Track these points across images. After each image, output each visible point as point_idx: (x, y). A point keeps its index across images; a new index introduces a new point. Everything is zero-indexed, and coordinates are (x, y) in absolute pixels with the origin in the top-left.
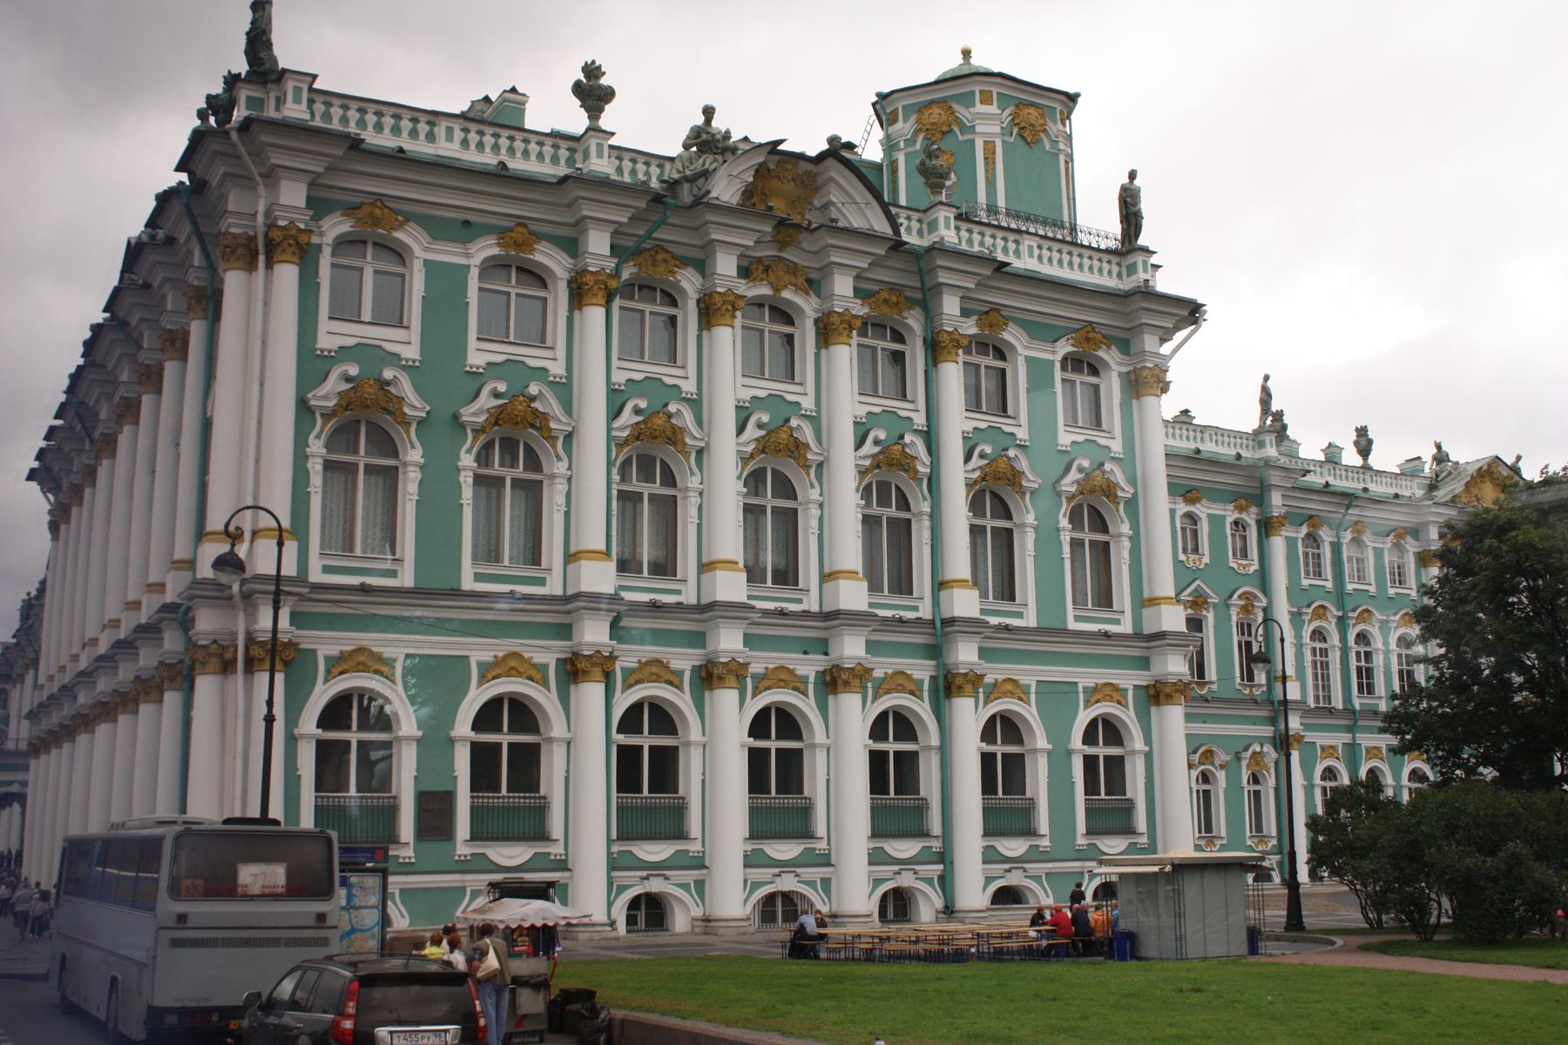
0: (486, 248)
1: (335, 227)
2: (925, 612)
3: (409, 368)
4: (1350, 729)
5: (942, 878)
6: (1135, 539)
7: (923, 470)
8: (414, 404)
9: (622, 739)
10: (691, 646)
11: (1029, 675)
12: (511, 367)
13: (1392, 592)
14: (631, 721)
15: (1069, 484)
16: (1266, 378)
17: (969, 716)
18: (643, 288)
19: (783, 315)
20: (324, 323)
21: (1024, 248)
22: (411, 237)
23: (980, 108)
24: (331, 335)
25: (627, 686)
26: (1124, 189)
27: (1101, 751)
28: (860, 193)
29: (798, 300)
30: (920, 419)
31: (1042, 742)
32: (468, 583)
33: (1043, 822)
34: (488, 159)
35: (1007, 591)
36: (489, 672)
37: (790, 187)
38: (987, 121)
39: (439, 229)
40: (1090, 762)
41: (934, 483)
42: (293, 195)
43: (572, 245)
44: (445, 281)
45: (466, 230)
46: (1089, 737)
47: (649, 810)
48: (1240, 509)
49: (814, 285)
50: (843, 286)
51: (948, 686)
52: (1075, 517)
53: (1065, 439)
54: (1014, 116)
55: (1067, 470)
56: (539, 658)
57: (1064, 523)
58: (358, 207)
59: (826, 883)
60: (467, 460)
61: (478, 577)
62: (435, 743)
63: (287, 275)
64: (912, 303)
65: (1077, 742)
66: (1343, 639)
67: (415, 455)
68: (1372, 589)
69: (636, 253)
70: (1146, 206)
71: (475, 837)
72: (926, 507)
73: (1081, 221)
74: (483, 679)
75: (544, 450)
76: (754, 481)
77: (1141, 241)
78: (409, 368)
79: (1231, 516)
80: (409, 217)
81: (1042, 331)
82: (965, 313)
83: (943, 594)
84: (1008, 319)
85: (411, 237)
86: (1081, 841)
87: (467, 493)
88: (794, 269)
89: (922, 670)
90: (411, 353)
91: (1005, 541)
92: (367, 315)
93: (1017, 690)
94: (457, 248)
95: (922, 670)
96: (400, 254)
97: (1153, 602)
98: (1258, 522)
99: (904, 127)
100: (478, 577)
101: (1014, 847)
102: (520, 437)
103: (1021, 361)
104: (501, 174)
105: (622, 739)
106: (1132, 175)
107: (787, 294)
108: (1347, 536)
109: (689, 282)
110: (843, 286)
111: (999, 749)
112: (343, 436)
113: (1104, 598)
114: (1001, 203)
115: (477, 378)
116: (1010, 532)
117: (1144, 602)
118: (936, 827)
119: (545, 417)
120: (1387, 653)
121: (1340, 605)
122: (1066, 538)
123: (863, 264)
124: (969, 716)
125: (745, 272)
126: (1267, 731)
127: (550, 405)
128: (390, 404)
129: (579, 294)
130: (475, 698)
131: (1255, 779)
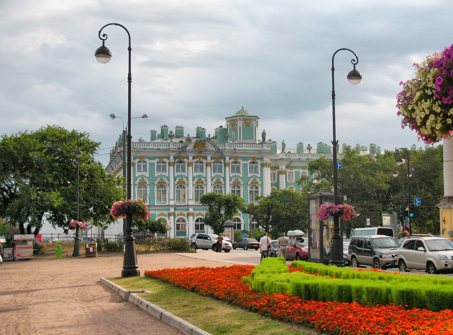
0: (157, 160)
3: (147, 178)
12: (161, 176)
14: (178, 221)
15: (249, 183)
18: (181, 162)
19: (201, 162)
22: (147, 160)
23: (239, 121)
30: (223, 176)
32: (156, 204)
36: (159, 215)
38: (240, 124)
39: (150, 158)
43: (169, 158)
44: (152, 165)
45: (154, 158)
47: (181, 232)
49: (205, 158)
50: (209, 158)
52: (252, 187)
56: (165, 213)
57: (249, 189)
60: (155, 189)
64: (221, 158)
67: (148, 189)
69: (178, 157)
72: (223, 189)
75: (166, 186)
76: (197, 187)
78: (147, 178)
80: (146, 157)
82: (230, 159)
84: (239, 158)
85: (147, 160)
87: (156, 193)
88: (202, 156)
90: (148, 175)
96: (146, 162)
102: (162, 185)
106: (264, 130)
107: (201, 160)
109: (186, 160)
110: (209, 158)
115: (157, 178)
122: (249, 191)
125: (194, 158)
127: (166, 180)
129: (170, 165)
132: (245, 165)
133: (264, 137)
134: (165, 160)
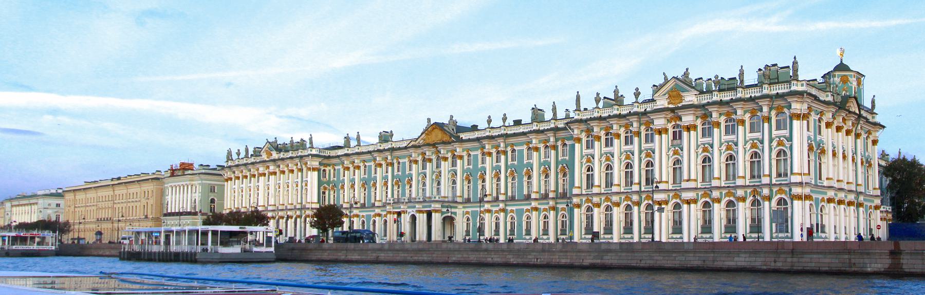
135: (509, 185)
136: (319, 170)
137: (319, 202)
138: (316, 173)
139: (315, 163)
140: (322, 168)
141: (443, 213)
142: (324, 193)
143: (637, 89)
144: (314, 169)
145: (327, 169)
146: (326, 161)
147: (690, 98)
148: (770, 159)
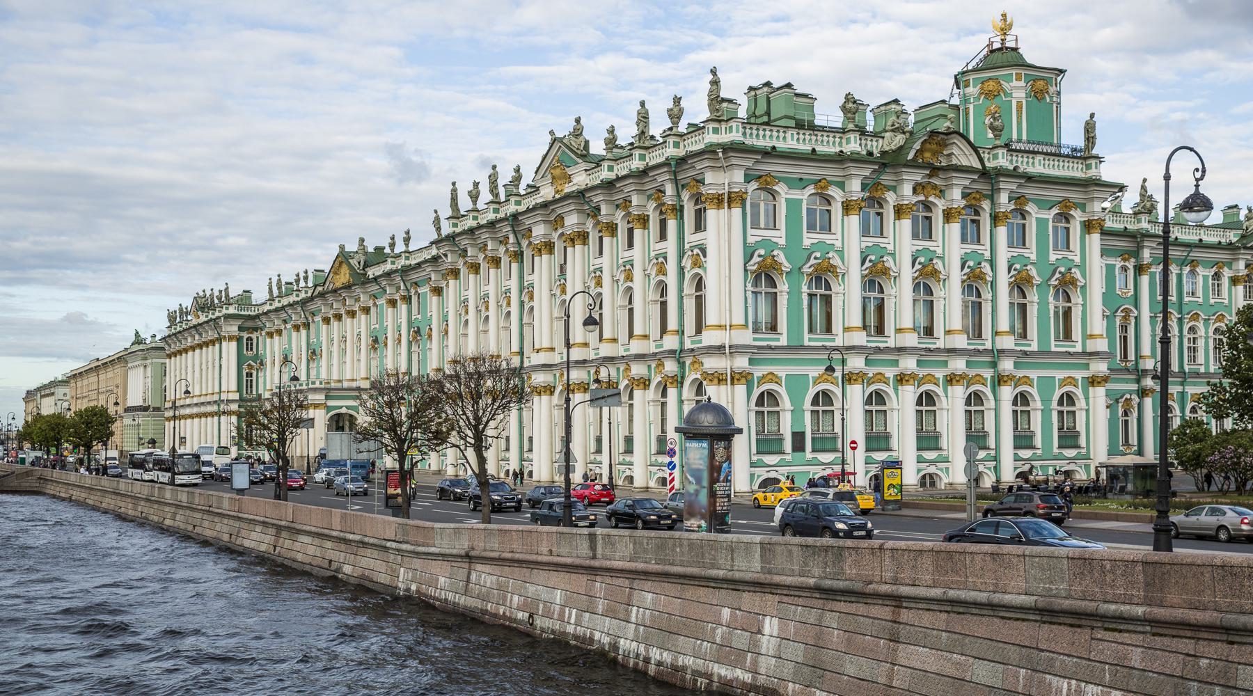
1: (754, 185)
2: (988, 345)
4: (1182, 384)
5: (995, 468)
6: (1084, 306)
7: (989, 279)
8: (787, 266)
9: (867, 407)
10: (892, 366)
11: (1034, 375)
13: (1212, 301)
15: (1054, 282)
16: (1145, 180)
17: (1007, 393)
20: (750, 231)
21: (1036, 161)
23: (1015, 83)
24: (754, 236)
25: (869, 384)
26: (1087, 123)
27: (1065, 409)
28: (968, 150)
29: (936, 201)
30: (987, 254)
31: (1039, 404)
32: (806, 343)
33: (1038, 441)
34: (807, 148)
35: (1024, 335)
37: (934, 147)
40: (1061, 413)
41: (993, 285)
42: (739, 176)
44: (793, 205)
45: (801, 183)
46: (1061, 403)
48: (1125, 260)
51: (999, 380)
53: (1053, 257)
54: (1032, 86)
55: (1054, 274)
57: (1051, 299)
58: (760, 177)
59: (947, 469)
61: (810, 340)
62: (797, 412)
63: (737, 212)
64: (986, 197)
65: (1054, 404)
66: (1181, 331)
68: (1200, 300)
70: (1098, 132)
71: (813, 451)
72: (989, 296)
73: (1063, 142)
74: (815, 383)
76: (916, 287)
77: (1094, 152)
79: (1118, 263)
81: (1045, 205)
83: (998, 338)
84: (1029, 200)
86: (1056, 451)
88: (935, 187)
89: (988, 374)
90: (782, 242)
91: (1023, 308)
92: (762, 226)
93: (1027, 380)
94: (799, 192)
95: (988, 374)
96: (773, 194)
97: (1091, 336)
98: (1135, 267)
99: (972, 90)
100: (810, 340)
101: (1025, 454)
103: (1034, 220)
104: (813, 157)
105: (867, 407)
106: (1092, 116)
107: (931, 199)
108: (1187, 269)
109: (891, 197)
111: (1019, 408)
112: (756, 282)
113: (1068, 335)
114: (1024, 138)
116: (1025, 305)
117: (1087, 337)
118: (992, 444)
119: (835, 267)
120: (1207, 338)
121: (1180, 312)
123: (967, 183)
124: (1007, 393)
126: (1134, 387)
127: (836, 261)
128: (776, 266)
129: (847, 208)
130: (811, 393)
131: (1126, 414)
132: (1041, 223)
133: (1090, 138)
134: (834, 192)
135: (415, 357)
136: (239, 340)
137: (239, 390)
138: (234, 344)
139: (233, 329)
140: (245, 335)
141: (328, 409)
142: (249, 375)
143: (517, 170)
144: (230, 338)
145: (254, 336)
146: (249, 324)
147: (580, 179)
148: (681, 298)
